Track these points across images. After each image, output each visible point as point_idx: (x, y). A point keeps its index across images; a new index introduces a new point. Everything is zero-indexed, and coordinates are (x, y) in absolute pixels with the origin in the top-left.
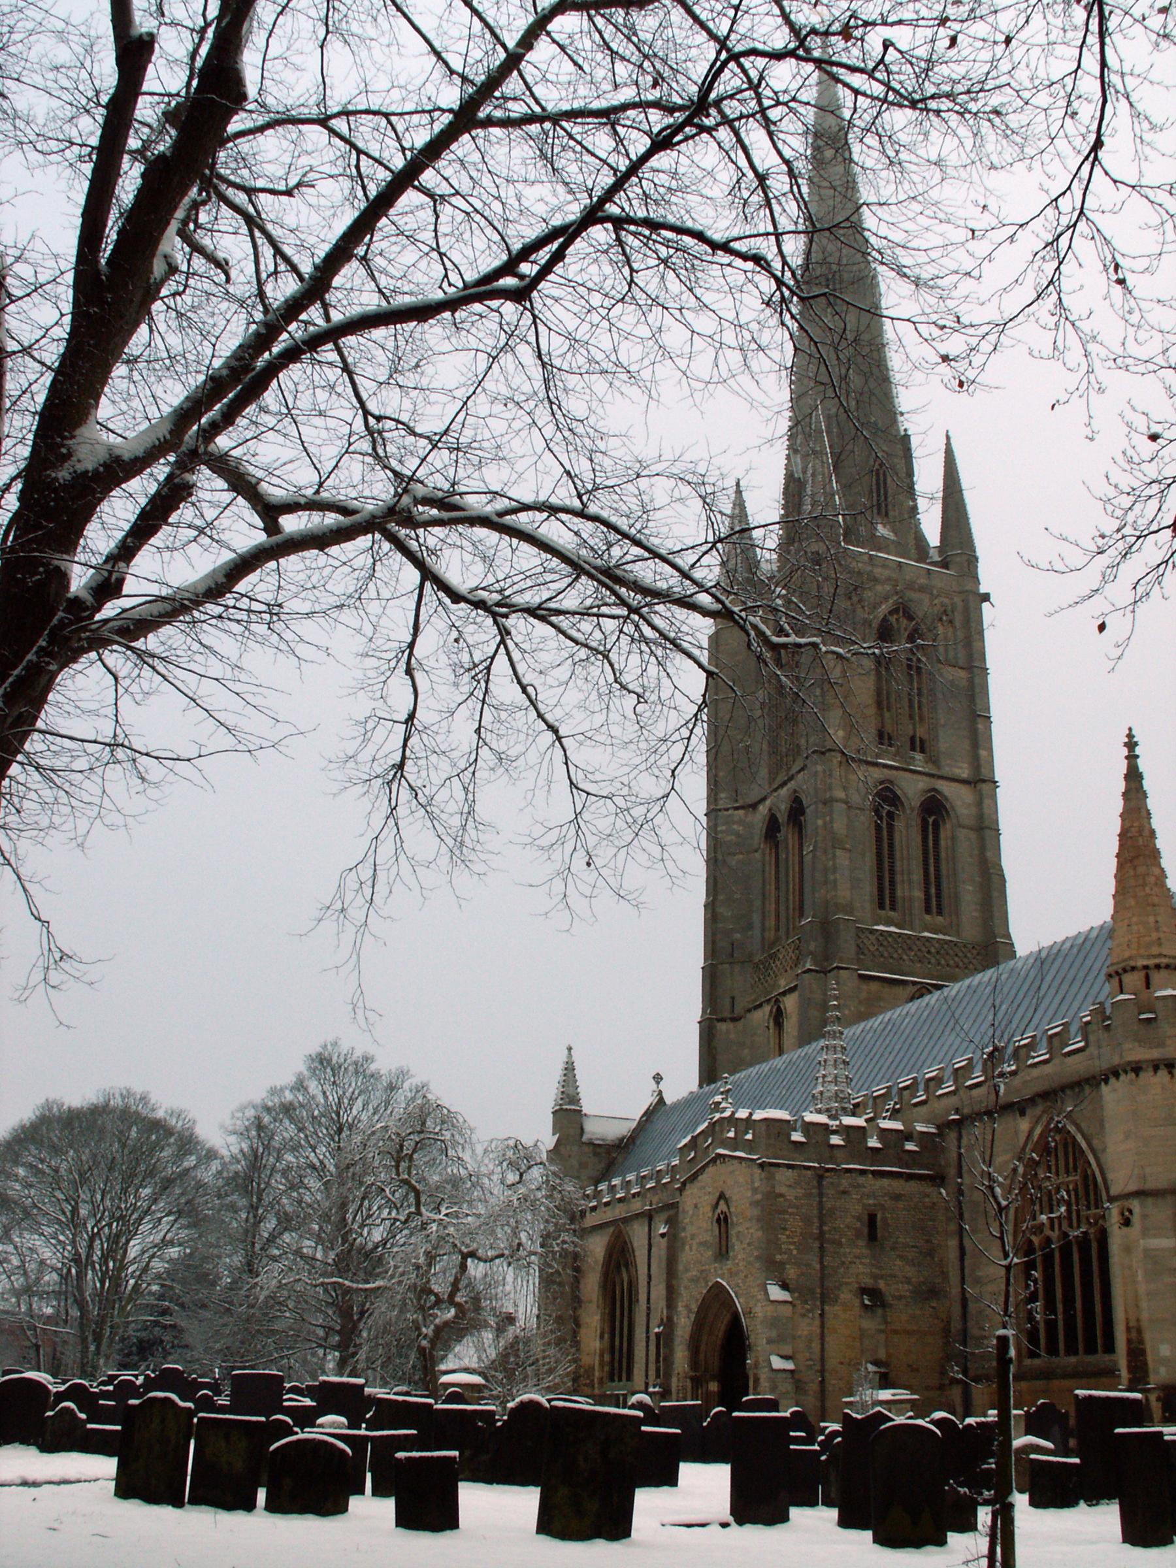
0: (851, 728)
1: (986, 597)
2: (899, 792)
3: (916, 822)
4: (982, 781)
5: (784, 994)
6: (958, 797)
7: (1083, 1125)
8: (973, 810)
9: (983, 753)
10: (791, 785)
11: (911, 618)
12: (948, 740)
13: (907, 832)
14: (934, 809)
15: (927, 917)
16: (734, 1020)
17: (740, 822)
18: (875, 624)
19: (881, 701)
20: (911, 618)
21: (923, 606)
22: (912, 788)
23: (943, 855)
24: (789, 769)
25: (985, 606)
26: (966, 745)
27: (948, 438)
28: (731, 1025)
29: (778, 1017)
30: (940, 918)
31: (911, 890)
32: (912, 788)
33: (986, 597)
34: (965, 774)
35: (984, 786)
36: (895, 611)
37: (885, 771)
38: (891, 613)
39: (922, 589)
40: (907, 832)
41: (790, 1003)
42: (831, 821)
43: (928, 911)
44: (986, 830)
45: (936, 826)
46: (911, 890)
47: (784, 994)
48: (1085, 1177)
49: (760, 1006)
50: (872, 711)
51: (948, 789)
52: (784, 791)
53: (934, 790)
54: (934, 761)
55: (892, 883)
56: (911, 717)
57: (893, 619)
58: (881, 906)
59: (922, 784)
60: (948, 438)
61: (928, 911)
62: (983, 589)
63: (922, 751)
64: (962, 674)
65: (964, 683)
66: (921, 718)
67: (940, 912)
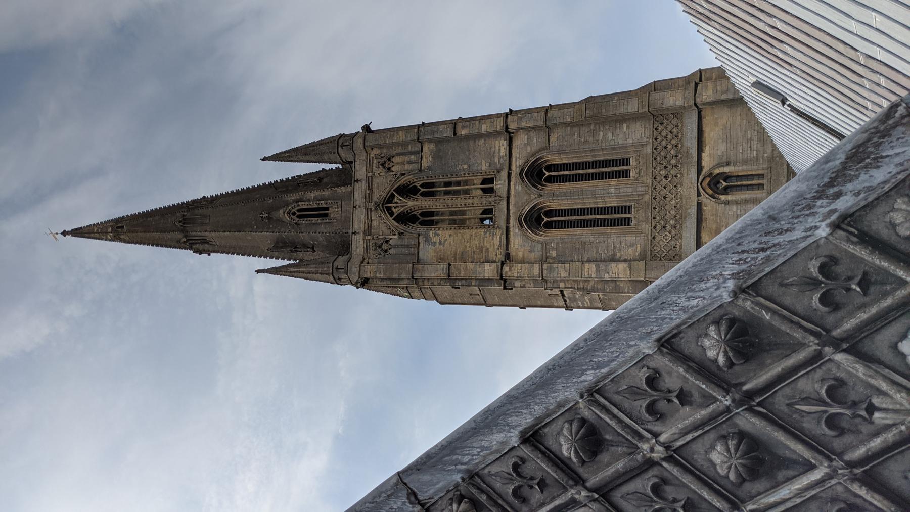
1: (366, 128)
2: (527, 209)
3: (550, 188)
4: (507, 125)
8: (533, 134)
11: (393, 196)
13: (560, 196)
14: (536, 174)
15: (632, 174)
18: (402, 227)
19: (457, 221)
21: (383, 185)
22: (523, 198)
25: (373, 128)
27: (265, 159)
30: (632, 161)
31: (609, 193)
32: (523, 198)
33: (366, 128)
34: (501, 145)
37: (512, 221)
38: (392, 214)
39: (370, 187)
40: (560, 196)
43: (625, 174)
44: (547, 119)
45: (550, 168)
46: (609, 193)
50: (467, 233)
53: (521, 174)
55: (604, 210)
56: (466, 192)
58: (627, 222)
59: (517, 186)
60: (265, 159)
61: (625, 174)
63: (491, 181)
66: (466, 183)
67: (626, 161)
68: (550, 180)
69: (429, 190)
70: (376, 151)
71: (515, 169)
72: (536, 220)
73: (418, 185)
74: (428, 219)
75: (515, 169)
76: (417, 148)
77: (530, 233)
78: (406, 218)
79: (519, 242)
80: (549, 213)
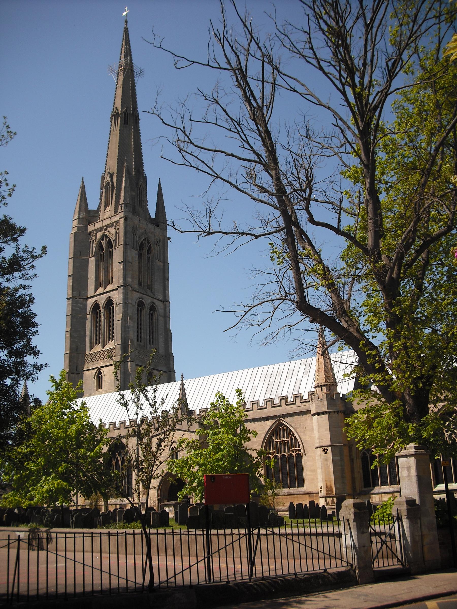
0: (133, 278)
1: (169, 239)
4: (166, 301)
5: (103, 367)
6: (159, 305)
7: (293, 425)
9: (167, 292)
10: (109, 294)
11: (149, 243)
12: (157, 286)
14: (153, 308)
16: (77, 374)
17: (81, 303)
20: (149, 243)
21: (152, 240)
22: (147, 301)
23: (154, 325)
24: (105, 289)
26: (162, 289)
27: (159, 180)
28: (76, 375)
29: (99, 376)
31: (146, 336)
34: (161, 298)
35: (167, 303)
36: (145, 239)
41: (103, 370)
42: (128, 310)
44: (166, 317)
46: (146, 336)
47: (103, 367)
48: (291, 439)
49: (90, 370)
51: (157, 303)
52: (105, 297)
54: (153, 293)
57: (144, 241)
58: (138, 341)
60: (159, 180)
62: (168, 236)
64: (162, 264)
65: (162, 267)
68: (149, 313)
69: (149, 259)
70: (162, 240)
71: (155, 301)
72: (141, 304)
73: (150, 255)
74: (140, 256)
75: (155, 301)
76: (162, 260)
77: (137, 301)
78: (141, 247)
79: (136, 295)
80: (141, 311)
